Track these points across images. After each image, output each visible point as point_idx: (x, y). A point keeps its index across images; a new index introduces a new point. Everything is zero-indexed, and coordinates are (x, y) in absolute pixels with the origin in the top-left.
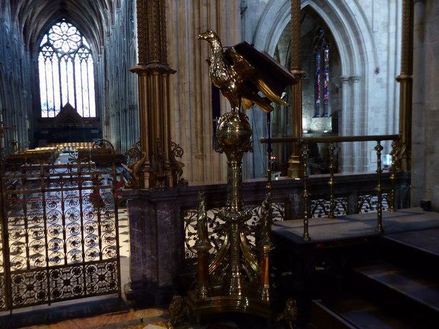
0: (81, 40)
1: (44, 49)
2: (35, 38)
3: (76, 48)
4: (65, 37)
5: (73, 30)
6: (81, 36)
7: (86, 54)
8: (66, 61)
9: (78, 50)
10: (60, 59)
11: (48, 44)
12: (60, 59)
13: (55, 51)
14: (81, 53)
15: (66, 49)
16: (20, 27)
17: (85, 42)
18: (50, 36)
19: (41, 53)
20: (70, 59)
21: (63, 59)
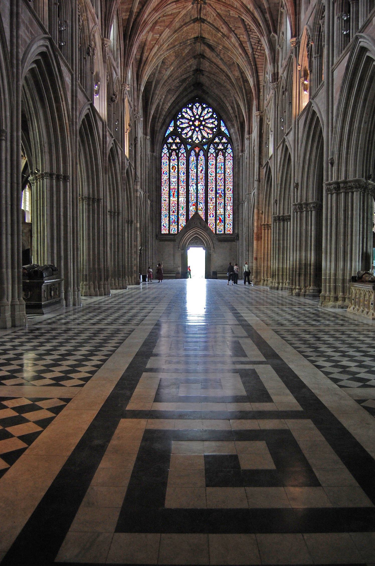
0: (219, 126)
1: (170, 140)
2: (159, 124)
3: (211, 136)
4: (197, 123)
5: (207, 113)
6: (219, 120)
7: (224, 143)
8: (197, 155)
11: (175, 133)
13: (184, 142)
14: (218, 144)
15: (197, 137)
16: (139, 90)
17: (223, 129)
19: (165, 146)
20: (202, 153)
21: (193, 153)
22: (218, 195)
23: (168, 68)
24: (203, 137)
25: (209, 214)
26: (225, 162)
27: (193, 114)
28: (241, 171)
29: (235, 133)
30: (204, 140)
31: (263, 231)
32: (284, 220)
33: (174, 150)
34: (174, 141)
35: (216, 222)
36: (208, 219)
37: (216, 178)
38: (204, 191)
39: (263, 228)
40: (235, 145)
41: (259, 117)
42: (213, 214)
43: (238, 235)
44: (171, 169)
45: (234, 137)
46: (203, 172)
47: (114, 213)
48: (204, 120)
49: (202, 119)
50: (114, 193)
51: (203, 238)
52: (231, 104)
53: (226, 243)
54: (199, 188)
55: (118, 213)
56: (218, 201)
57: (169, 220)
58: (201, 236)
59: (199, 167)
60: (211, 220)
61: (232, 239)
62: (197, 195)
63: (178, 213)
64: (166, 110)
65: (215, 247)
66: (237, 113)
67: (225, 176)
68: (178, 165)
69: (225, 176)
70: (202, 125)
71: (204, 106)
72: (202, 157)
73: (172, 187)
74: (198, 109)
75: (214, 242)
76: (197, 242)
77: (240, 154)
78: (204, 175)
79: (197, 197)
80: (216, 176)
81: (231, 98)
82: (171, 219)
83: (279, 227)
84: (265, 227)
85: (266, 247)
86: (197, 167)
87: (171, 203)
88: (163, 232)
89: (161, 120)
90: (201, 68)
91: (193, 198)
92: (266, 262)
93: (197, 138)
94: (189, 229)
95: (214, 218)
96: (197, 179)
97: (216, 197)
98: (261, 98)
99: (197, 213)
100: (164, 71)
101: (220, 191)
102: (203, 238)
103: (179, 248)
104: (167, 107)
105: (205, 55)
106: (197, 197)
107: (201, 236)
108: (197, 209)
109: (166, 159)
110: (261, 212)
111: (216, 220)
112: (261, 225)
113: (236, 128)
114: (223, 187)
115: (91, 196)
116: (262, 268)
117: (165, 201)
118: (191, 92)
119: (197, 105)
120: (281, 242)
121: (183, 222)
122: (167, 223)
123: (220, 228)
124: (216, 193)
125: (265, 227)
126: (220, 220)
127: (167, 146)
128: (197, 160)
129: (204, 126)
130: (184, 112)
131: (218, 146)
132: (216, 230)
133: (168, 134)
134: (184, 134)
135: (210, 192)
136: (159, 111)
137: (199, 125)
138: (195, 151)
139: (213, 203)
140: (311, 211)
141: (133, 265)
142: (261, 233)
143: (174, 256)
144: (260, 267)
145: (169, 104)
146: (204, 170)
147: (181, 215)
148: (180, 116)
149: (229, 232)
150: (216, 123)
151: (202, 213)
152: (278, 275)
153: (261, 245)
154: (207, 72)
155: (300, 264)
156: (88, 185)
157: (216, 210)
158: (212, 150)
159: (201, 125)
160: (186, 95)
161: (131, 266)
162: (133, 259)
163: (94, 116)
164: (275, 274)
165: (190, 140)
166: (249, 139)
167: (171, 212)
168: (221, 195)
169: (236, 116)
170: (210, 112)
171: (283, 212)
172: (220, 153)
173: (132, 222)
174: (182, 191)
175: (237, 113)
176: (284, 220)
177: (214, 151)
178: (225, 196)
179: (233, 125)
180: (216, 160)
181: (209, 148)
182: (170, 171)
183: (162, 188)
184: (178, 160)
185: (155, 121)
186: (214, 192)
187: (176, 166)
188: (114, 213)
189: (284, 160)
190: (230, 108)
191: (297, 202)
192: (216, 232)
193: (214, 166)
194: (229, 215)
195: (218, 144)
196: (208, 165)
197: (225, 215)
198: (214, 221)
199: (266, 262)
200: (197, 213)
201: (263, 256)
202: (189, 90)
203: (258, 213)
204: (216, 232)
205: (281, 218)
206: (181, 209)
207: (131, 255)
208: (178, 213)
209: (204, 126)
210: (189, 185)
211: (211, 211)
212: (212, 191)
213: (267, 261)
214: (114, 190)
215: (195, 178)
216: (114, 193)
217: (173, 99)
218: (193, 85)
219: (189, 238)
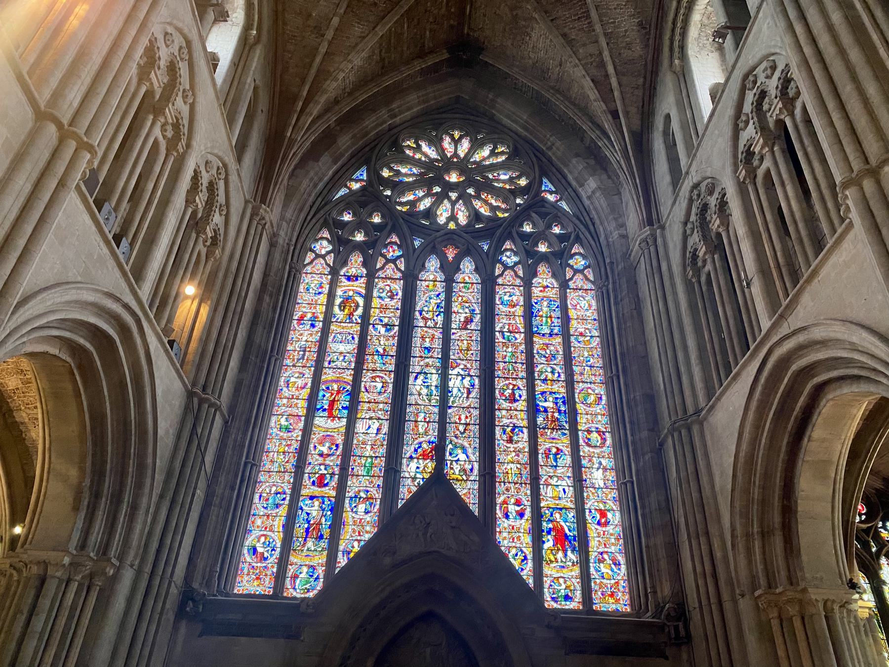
8: (450, 271)
14: (533, 238)
20: (467, 265)
21: (433, 263)
22: (540, 420)
25: (500, 500)
38: (474, 400)
42: (518, 503)
44: (336, 310)
46: (473, 326)
54: (454, 383)
56: (544, 445)
59: (455, 307)
63: (341, 488)
68: (368, 298)
73: (328, 375)
78: (476, 336)
80: (529, 343)
87: (315, 438)
95: (525, 524)
101: (549, 404)
114: (560, 389)
122: (277, 538)
124: (533, 409)
126: (561, 538)
128: (449, 282)
133: (342, 196)
135: (505, 405)
139: (518, 452)
146: (477, 318)
163: (200, 469)
167: (306, 481)
172: (542, 268)
177: (515, 259)
181: (498, 250)
183: (284, 375)
186: (522, 405)
187: (361, 301)
195: (533, 238)
198: (527, 539)
206: (362, 471)
208: (341, 488)
212: (513, 399)
215: (437, 344)
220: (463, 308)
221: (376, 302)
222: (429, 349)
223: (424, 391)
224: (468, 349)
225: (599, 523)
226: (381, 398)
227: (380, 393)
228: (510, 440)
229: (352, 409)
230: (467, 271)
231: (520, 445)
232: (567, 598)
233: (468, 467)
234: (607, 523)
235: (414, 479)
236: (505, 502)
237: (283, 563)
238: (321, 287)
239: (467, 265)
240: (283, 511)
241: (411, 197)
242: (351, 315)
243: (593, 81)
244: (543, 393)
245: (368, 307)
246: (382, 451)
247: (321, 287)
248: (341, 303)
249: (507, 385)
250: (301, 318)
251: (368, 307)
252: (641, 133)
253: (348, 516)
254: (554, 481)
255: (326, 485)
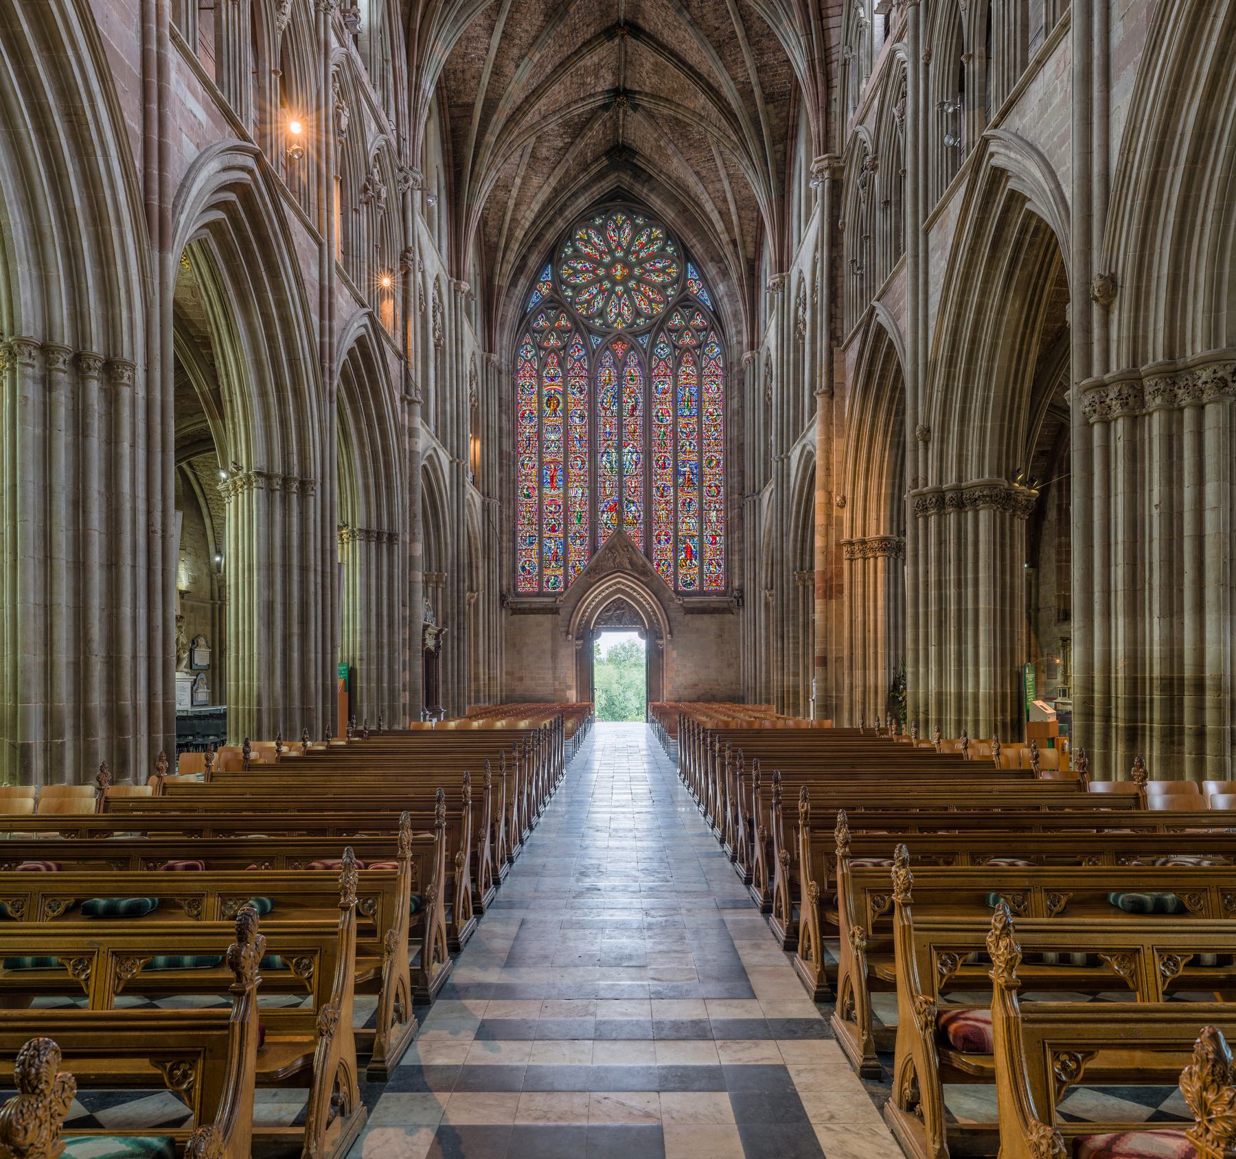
0: (681, 280)
8: (620, 364)
9: (668, 316)
10: (594, 356)
11: (555, 303)
12: (594, 356)
13: (581, 327)
14: (679, 331)
15: (618, 315)
17: (695, 288)
18: (565, 272)
20: (633, 359)
21: (607, 359)
23: (522, 57)
24: (638, 313)
26: (700, 385)
27: (608, 245)
28: (748, 405)
29: (731, 295)
30: (641, 321)
31: (846, 564)
32: (960, 506)
33: (554, 351)
34: (552, 323)
35: (676, 560)
36: (652, 549)
37: (674, 432)
39: (846, 555)
40: (731, 330)
41: (826, 174)
43: (741, 597)
45: (727, 308)
46: (637, 413)
47: (286, 480)
48: (640, 262)
49: (633, 259)
50: (282, 401)
51: (638, 603)
52: (719, 204)
53: (706, 617)
54: (627, 458)
55: (304, 485)
57: (540, 553)
58: (634, 599)
60: (663, 550)
61: (726, 605)
62: (620, 481)
63: (566, 531)
64: (527, 225)
65: (675, 632)
66: (736, 230)
67: (700, 422)
68: (564, 394)
69: (700, 422)
70: (635, 276)
71: (640, 221)
72: (633, 370)
74: (621, 231)
75: (672, 615)
76: (619, 616)
77: (747, 355)
79: (621, 486)
81: (718, 186)
82: (545, 550)
83: (939, 533)
84: (852, 553)
85: (860, 619)
86: (618, 398)
88: (524, 587)
89: (511, 256)
90: (628, 87)
91: (608, 490)
92: (858, 674)
93: (619, 315)
94: (598, 577)
96: (620, 434)
97: (676, 486)
98: (836, 108)
99: (619, 532)
100: (509, 68)
102: (638, 603)
103: (568, 633)
104: (530, 216)
105: (640, 22)
106: (621, 486)
107: (634, 599)
108: (621, 520)
109: (531, 376)
110: (837, 499)
111: (676, 551)
112: (839, 546)
113: (734, 276)
114: (694, 457)
115: (64, 336)
116: (846, 694)
117: (528, 496)
118: (601, 176)
119: (620, 218)
120: (952, 591)
121: (578, 556)
122: (535, 561)
123: (689, 572)
124: (677, 473)
125: (852, 553)
126: (689, 552)
127: (533, 339)
129: (640, 280)
130: (581, 239)
131: (681, 337)
132: (676, 579)
134: (581, 304)
136: (506, 226)
137: (623, 276)
138: (614, 353)
139: (667, 503)
140: (1200, 409)
141: (399, 685)
142: (840, 574)
143: (554, 655)
144: (839, 688)
145: (536, 207)
147: (575, 538)
148: (569, 251)
149: (713, 587)
150: (673, 271)
151: (634, 533)
152: (940, 722)
153: (840, 615)
154: (646, 94)
155: (1135, 683)
156: (44, 281)
157: (676, 524)
158: (663, 350)
159: (631, 276)
160: (586, 187)
161: (392, 691)
162: (398, 667)
164: (927, 721)
165: (598, 322)
166: (782, 286)
168: (690, 480)
169: (734, 242)
170: (657, 238)
171: (960, 471)
172: (687, 357)
173: (392, 537)
174: (578, 469)
175: (736, 230)
176: (960, 506)
178: (701, 482)
179: (724, 273)
180: (676, 377)
181: (653, 345)
182: (540, 410)
184: (565, 377)
185: (495, 259)
186: (669, 471)
188: (286, 480)
189: (973, 250)
190: (715, 216)
191: (1106, 368)
192: (676, 585)
193: (669, 396)
194: (714, 537)
196: (650, 393)
197: (701, 536)
198: (670, 555)
199: (858, 674)
200: (619, 532)
201: (846, 653)
202: (594, 169)
203: (829, 503)
204: (676, 585)
205: (949, 495)
207: (391, 652)
208: (566, 531)
209: (640, 280)
210: (596, 452)
211: (662, 529)
213: (864, 668)
214: (280, 388)
216: (282, 401)
217: (546, 191)
218: (607, 153)
219: (600, 603)
220: (630, 397)
221: (570, 398)
222: (610, 434)
223: (608, 466)
224: (635, 431)
225: (712, 544)
226: (582, 472)
227: (580, 469)
228: (662, 496)
229: (566, 481)
230: (632, 364)
231: (668, 498)
232: (691, 584)
233: (637, 514)
234: (715, 543)
235: (606, 524)
236: (659, 535)
237: (540, 574)
238: (532, 388)
239: (633, 359)
240: (535, 547)
241: (586, 296)
242: (555, 410)
243: (720, 212)
244: (684, 462)
245: (566, 403)
246: (586, 508)
247: (532, 388)
248: (548, 400)
249: (661, 457)
250: (523, 414)
251: (566, 403)
252: (754, 260)
253: (572, 548)
254: (687, 520)
255: (555, 531)
